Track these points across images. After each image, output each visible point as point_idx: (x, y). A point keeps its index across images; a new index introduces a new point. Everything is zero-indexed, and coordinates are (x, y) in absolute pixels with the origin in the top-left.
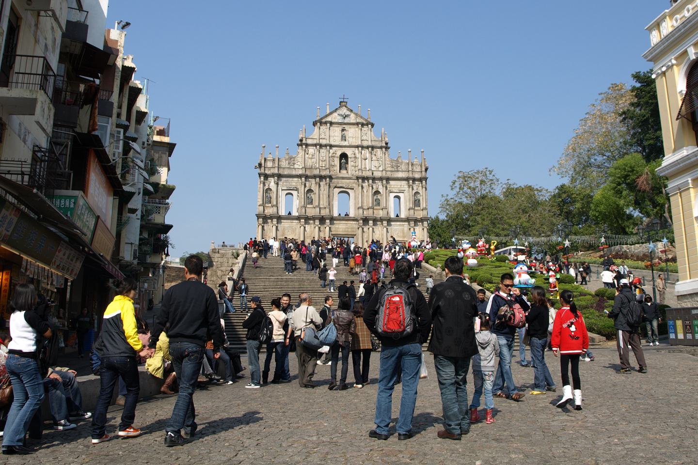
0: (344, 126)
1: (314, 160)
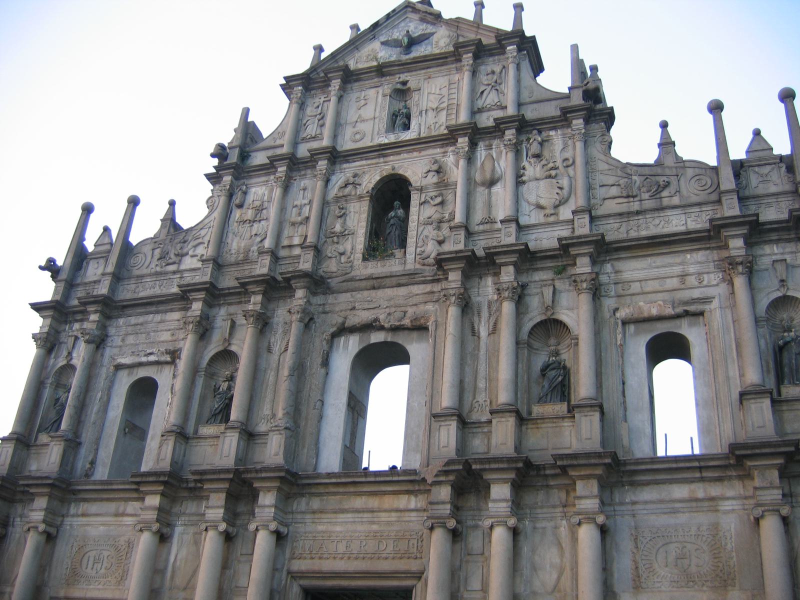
0: (403, 77)
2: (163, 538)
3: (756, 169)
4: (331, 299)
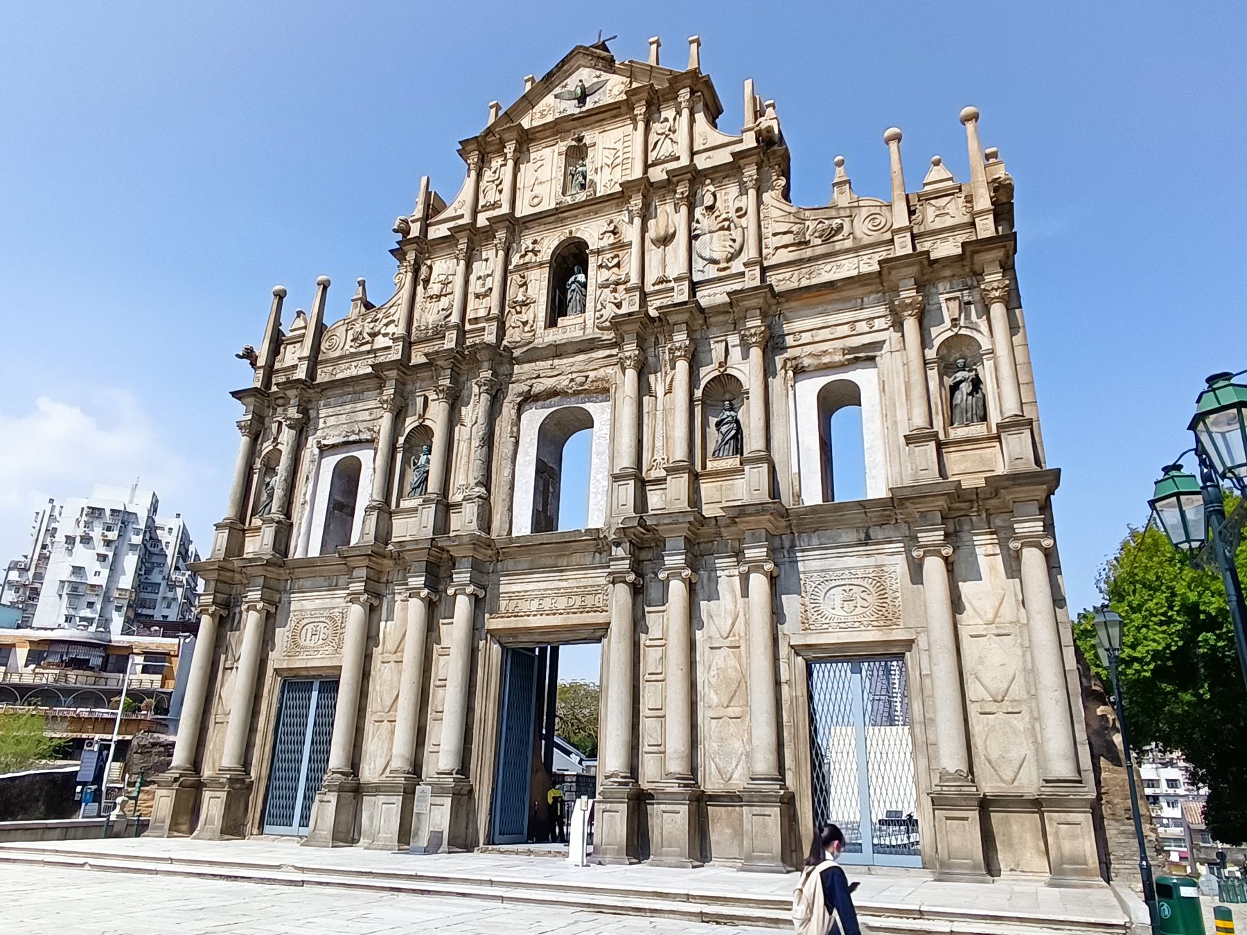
1: (444, 302)
3: (933, 202)
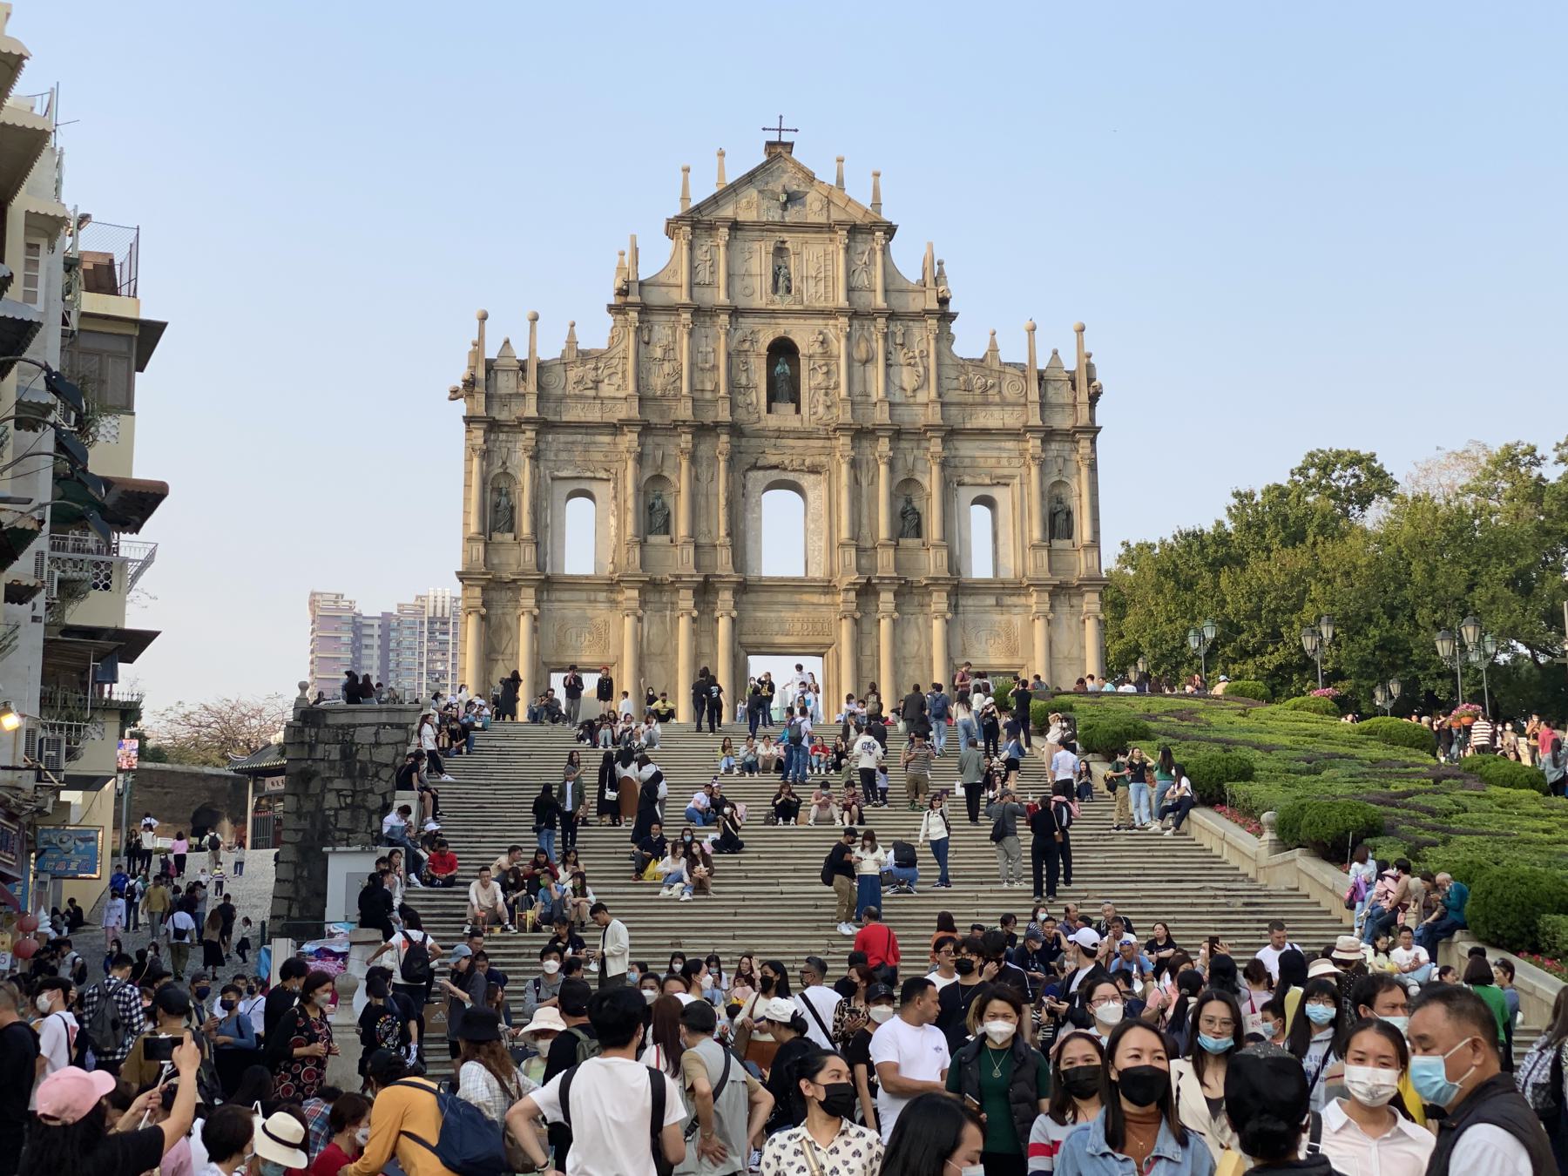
0: (785, 236)
2: (640, 619)
4: (744, 441)
